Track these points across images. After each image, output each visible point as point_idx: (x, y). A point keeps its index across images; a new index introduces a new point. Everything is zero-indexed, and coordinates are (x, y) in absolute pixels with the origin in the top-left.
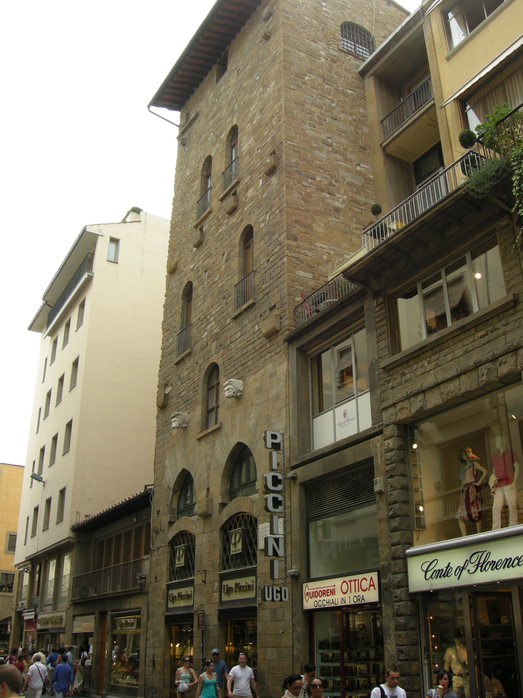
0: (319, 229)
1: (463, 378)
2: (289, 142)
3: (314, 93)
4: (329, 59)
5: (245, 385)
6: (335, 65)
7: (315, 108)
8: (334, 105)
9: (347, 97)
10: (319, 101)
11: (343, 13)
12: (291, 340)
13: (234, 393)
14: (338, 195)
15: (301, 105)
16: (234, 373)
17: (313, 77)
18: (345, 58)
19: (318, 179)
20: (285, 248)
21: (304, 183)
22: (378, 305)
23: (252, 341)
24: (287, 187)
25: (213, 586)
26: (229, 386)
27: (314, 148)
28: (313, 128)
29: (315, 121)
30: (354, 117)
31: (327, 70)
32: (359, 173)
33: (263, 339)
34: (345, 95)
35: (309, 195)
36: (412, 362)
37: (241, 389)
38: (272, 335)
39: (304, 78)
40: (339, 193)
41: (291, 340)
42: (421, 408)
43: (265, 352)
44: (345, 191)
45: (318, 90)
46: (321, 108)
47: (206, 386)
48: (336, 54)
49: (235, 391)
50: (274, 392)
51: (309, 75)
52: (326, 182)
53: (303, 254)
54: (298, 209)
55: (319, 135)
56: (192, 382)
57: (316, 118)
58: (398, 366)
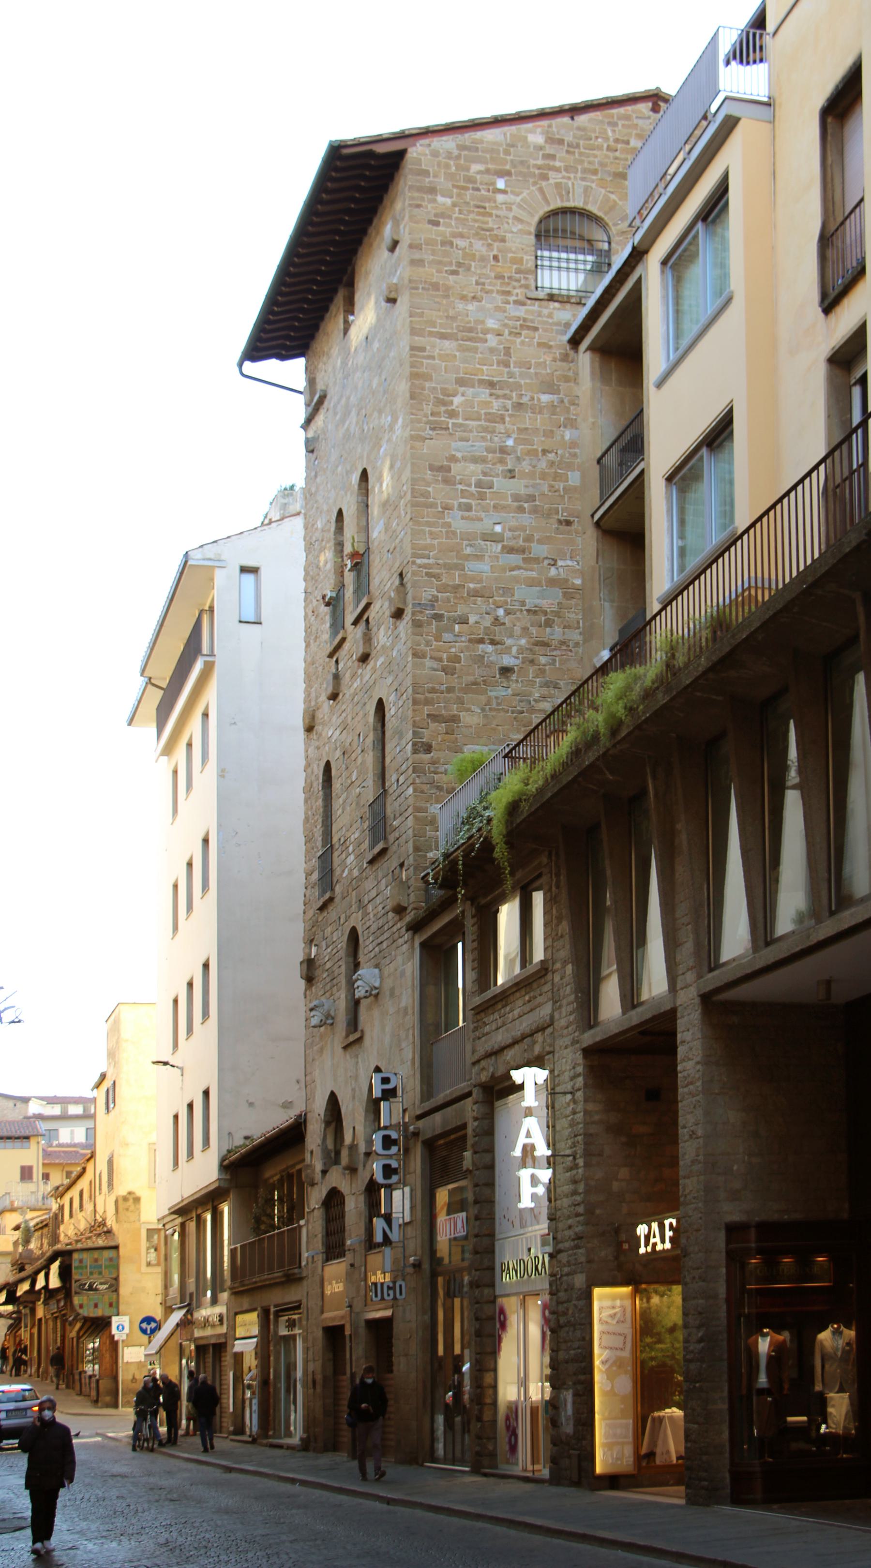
0: (471, 719)
1: (516, 1046)
2: (419, 561)
3: (471, 431)
4: (507, 332)
5: (381, 978)
6: (518, 340)
7: (472, 467)
8: (510, 443)
9: (540, 413)
10: (479, 447)
11: (541, 190)
12: (415, 927)
13: (367, 991)
14: (509, 642)
15: (442, 469)
16: (372, 954)
17: (470, 391)
18: (539, 315)
19: (472, 619)
20: (411, 769)
21: (447, 636)
22: (473, 917)
24: (413, 654)
26: (367, 975)
27: (467, 557)
28: (467, 514)
29: (471, 495)
30: (551, 456)
31: (499, 363)
32: (553, 582)
33: (391, 915)
34: (537, 409)
35: (456, 659)
36: (490, 1011)
37: (377, 984)
38: (400, 910)
39: (452, 403)
40: (511, 636)
41: (415, 927)
42: (493, 1074)
43: (396, 935)
44: (525, 629)
45: (480, 420)
46: (483, 460)
47: (351, 960)
48: (521, 311)
49: (367, 989)
50: (403, 1004)
51: (462, 389)
52: (487, 622)
53: (442, 773)
54: (433, 690)
55: (477, 528)
57: (473, 489)
58: (482, 1011)
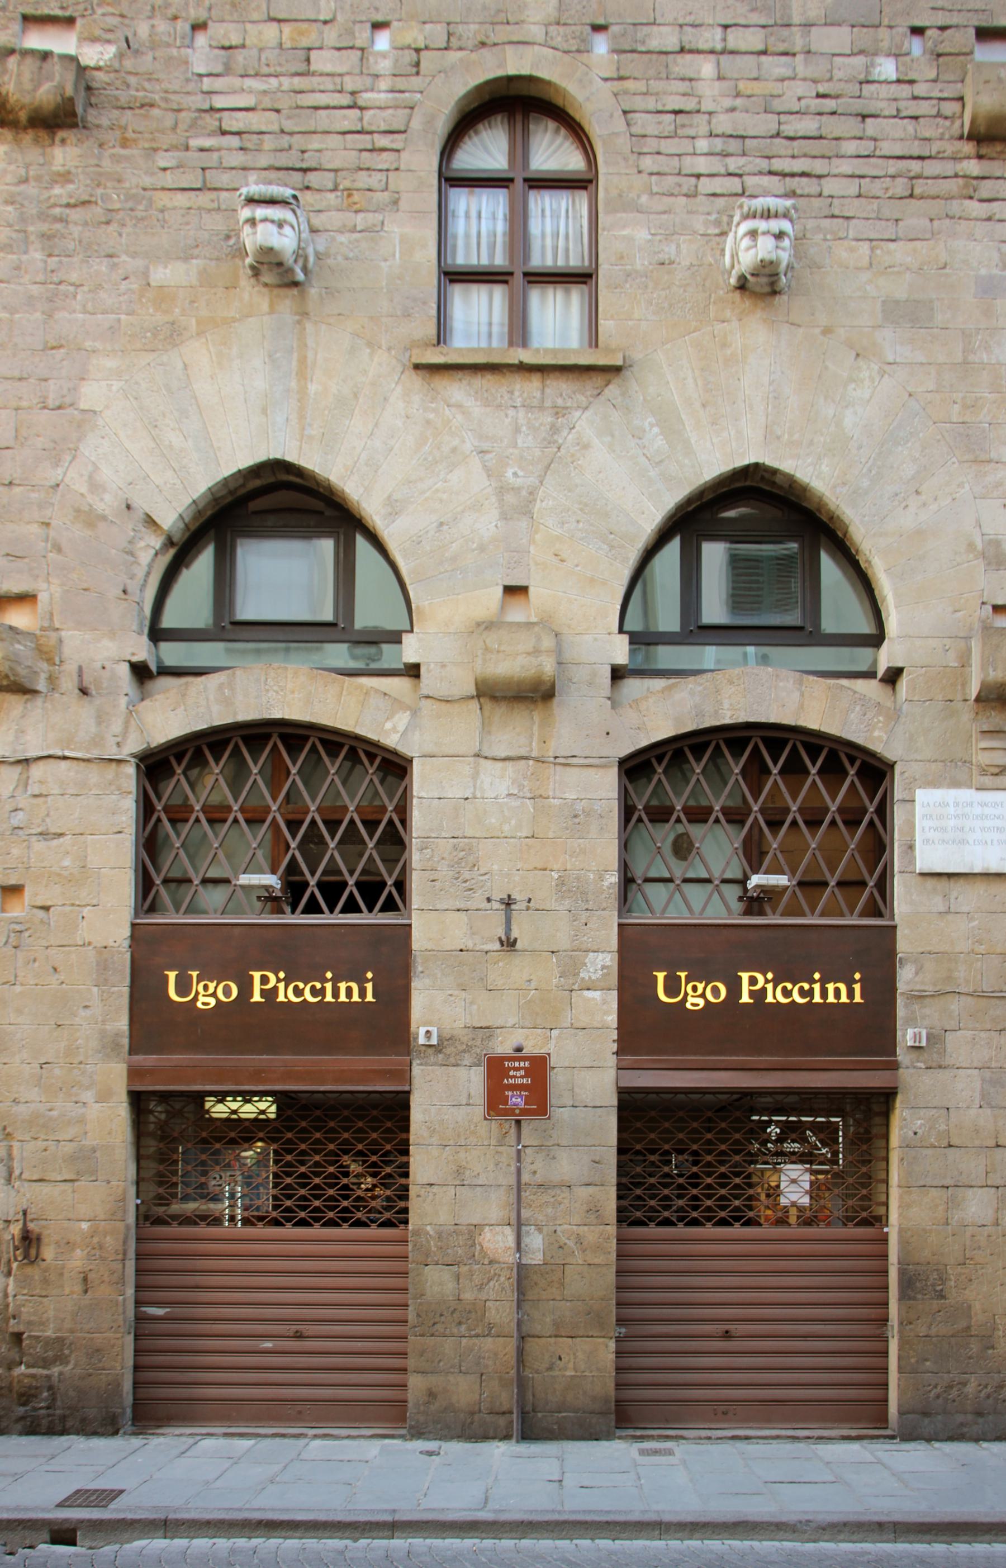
23: (858, 106)
25: (571, 968)
56: (345, 100)
